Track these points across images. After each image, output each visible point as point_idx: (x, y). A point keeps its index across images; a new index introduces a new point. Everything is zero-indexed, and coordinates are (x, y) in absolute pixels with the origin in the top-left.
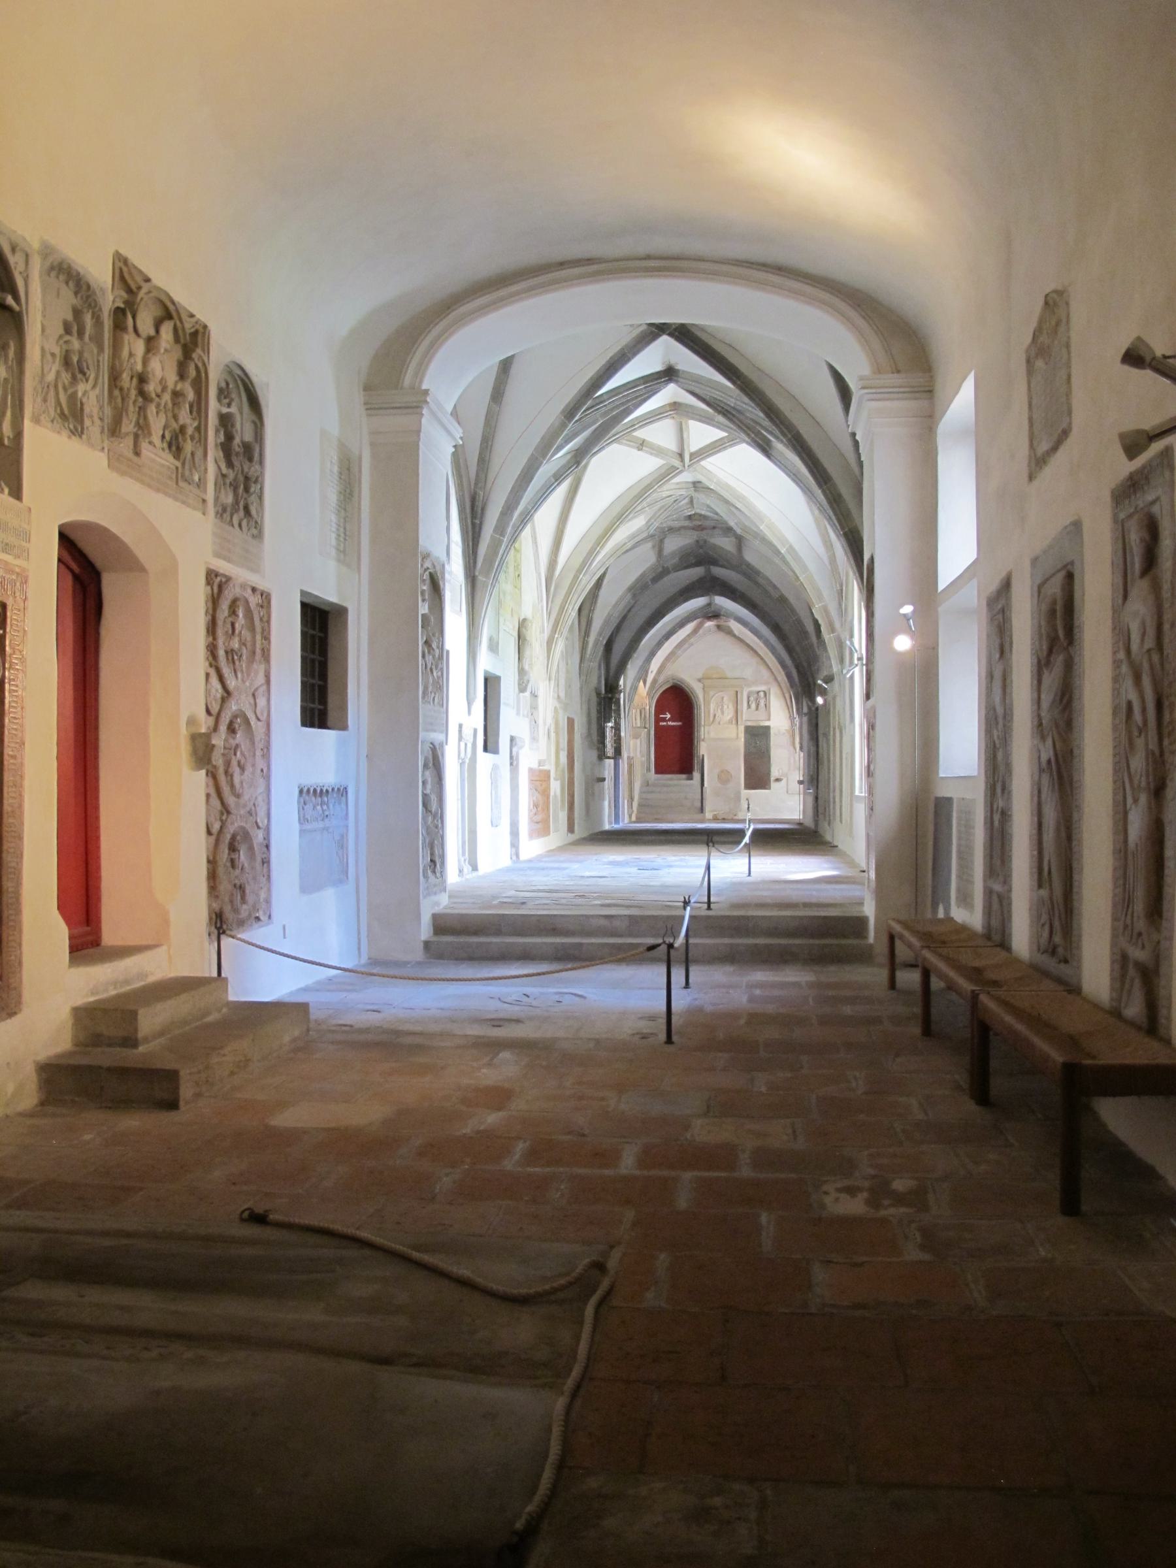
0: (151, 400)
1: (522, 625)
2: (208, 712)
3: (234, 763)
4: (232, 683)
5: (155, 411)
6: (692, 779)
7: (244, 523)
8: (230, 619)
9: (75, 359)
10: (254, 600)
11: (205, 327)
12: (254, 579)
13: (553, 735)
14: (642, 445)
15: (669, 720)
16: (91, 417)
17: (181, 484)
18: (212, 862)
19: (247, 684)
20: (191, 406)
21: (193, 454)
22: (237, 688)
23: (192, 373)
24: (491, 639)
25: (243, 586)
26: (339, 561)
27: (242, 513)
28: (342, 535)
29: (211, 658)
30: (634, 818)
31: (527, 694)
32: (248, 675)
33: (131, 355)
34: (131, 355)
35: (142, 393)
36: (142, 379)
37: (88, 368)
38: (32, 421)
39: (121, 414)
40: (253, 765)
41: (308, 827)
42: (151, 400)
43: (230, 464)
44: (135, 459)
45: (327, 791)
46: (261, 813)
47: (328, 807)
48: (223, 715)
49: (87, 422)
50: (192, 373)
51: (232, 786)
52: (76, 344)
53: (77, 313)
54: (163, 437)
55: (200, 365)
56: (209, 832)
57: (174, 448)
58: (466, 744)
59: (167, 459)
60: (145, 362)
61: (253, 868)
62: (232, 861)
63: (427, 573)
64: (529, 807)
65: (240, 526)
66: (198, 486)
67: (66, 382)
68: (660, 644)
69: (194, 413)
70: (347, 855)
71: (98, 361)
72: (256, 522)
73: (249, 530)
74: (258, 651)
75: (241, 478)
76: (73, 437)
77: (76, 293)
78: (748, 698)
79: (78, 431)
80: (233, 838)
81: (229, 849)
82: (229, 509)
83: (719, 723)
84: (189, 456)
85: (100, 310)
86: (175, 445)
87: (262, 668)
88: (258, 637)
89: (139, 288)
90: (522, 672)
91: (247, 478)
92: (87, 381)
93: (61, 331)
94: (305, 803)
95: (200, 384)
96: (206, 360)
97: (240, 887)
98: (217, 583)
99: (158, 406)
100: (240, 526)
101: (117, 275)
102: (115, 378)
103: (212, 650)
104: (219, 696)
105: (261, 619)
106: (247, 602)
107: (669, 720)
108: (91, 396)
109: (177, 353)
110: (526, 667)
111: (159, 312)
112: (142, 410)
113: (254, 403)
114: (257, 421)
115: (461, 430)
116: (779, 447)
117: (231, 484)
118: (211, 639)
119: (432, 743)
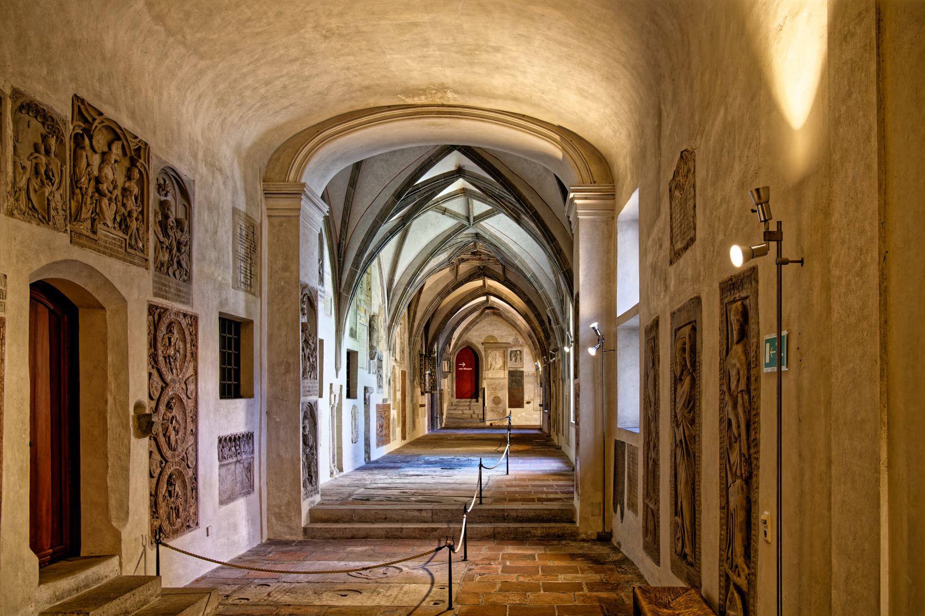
0: (105, 196)
1: (372, 319)
2: (151, 397)
3: (171, 428)
4: (169, 377)
5: (107, 202)
8: (167, 336)
9: (42, 170)
10: (184, 323)
11: (146, 144)
12: (183, 308)
15: (465, 367)
16: (56, 209)
17: (128, 250)
18: (154, 496)
19: (180, 376)
21: (138, 229)
22: (173, 381)
23: (136, 175)
24: (351, 329)
25: (177, 313)
26: (246, 291)
27: (175, 266)
28: (249, 275)
29: (153, 363)
31: (376, 360)
32: (181, 370)
33: (88, 165)
35: (98, 190)
36: (98, 181)
37: (53, 176)
40: (185, 428)
41: (226, 462)
42: (105, 196)
43: (166, 235)
44: (92, 236)
45: (239, 437)
46: (191, 459)
48: (162, 398)
49: (53, 213)
50: (136, 175)
51: (169, 444)
52: (43, 159)
53: (44, 138)
54: (115, 219)
55: (142, 170)
56: (151, 476)
57: (123, 227)
58: (335, 395)
61: (185, 494)
62: (170, 492)
65: (174, 275)
66: (143, 251)
68: (458, 324)
69: (139, 202)
71: (62, 170)
72: (186, 271)
73: (181, 277)
74: (188, 354)
75: (174, 244)
76: (41, 224)
77: (43, 124)
79: (45, 219)
80: (170, 476)
81: (167, 484)
82: (166, 264)
84: (135, 231)
85: (63, 135)
86: (123, 224)
87: (192, 365)
88: (188, 345)
89: (94, 120)
90: (372, 347)
91: (179, 243)
92: (53, 185)
93: (33, 151)
94: (223, 447)
95: (142, 182)
97: (175, 508)
98: (156, 314)
99: (110, 200)
100: (174, 275)
102: (75, 182)
103: (153, 358)
104: (159, 387)
105: (191, 334)
106: (180, 323)
107: (465, 367)
109: (126, 163)
110: (375, 344)
111: (110, 137)
112: (98, 202)
113: (185, 194)
114: (186, 204)
117: (167, 247)
118: (153, 350)
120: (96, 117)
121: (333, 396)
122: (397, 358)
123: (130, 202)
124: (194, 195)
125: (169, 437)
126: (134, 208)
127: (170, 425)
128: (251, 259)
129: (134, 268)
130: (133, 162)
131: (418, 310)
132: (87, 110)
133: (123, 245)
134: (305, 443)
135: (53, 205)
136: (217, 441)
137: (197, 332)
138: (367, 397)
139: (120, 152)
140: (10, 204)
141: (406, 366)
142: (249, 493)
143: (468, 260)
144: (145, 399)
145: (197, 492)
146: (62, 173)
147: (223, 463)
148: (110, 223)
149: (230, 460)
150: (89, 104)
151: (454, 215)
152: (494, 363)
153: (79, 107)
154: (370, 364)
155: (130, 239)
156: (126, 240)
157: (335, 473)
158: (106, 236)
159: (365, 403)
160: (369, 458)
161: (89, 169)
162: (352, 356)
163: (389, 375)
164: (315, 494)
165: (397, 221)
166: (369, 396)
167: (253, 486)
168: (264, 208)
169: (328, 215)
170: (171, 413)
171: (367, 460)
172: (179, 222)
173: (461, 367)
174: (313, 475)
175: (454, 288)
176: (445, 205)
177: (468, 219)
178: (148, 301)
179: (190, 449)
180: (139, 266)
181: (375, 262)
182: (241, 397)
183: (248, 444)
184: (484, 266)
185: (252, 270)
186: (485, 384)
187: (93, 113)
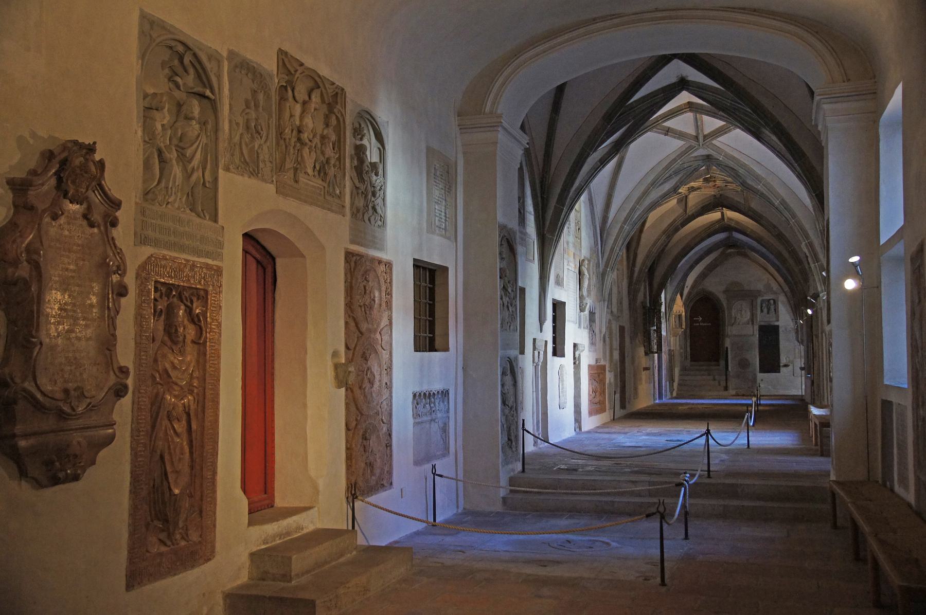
0: (306, 144)
2: (347, 347)
3: (366, 381)
5: (308, 150)
6: (719, 365)
7: (372, 219)
11: (343, 89)
13: (607, 339)
14: (668, 131)
16: (264, 161)
17: (328, 198)
20: (334, 144)
23: (333, 121)
27: (371, 211)
29: (349, 312)
30: (675, 394)
33: (291, 116)
34: (291, 116)
35: (299, 139)
37: (262, 130)
38: (224, 170)
39: (285, 159)
40: (380, 381)
44: (295, 185)
47: (435, 405)
49: (261, 166)
50: (333, 121)
52: (253, 115)
53: (254, 92)
54: (315, 167)
55: (339, 115)
57: (322, 174)
58: (539, 352)
59: (318, 182)
60: (302, 118)
63: (505, 239)
64: (589, 393)
66: (339, 197)
69: (336, 148)
70: (449, 437)
71: (268, 124)
72: (381, 216)
76: (252, 176)
78: (762, 304)
79: (255, 173)
81: (363, 438)
83: (739, 324)
85: (270, 89)
86: (322, 171)
89: (296, 71)
92: (261, 138)
94: (417, 404)
95: (339, 130)
96: (344, 113)
100: (369, 220)
101: (281, 63)
102: (280, 134)
103: (349, 306)
108: (264, 148)
109: (324, 110)
111: (311, 84)
115: (527, 138)
116: (767, 132)
119: (508, 358)
120: (298, 68)
121: (536, 353)
122: (613, 310)
123: (328, 149)
124: (388, 137)
126: (332, 155)
127: (365, 377)
128: (446, 200)
129: (331, 215)
130: (331, 109)
131: (638, 252)
132: (289, 61)
133: (322, 193)
134: (504, 403)
135: (261, 157)
136: (411, 396)
137: (391, 280)
138: (577, 356)
139: (319, 100)
140: (227, 159)
141: (625, 321)
143: (699, 188)
145: (391, 449)
146: (269, 126)
147: (417, 421)
148: (310, 171)
149: (425, 418)
150: (291, 56)
151: (680, 135)
152: (739, 316)
153: (283, 60)
154: (580, 317)
155: (329, 186)
156: (324, 187)
158: (307, 184)
159: (574, 363)
161: (292, 120)
162: (559, 307)
163: (604, 330)
164: (516, 461)
165: (609, 147)
166: (580, 355)
167: (449, 448)
168: (459, 143)
169: (528, 146)
172: (374, 166)
173: (697, 321)
174: (513, 438)
175: (684, 224)
176: (668, 124)
177: (697, 138)
178: (345, 248)
179: (385, 403)
180: (336, 213)
181: (584, 198)
182: (436, 351)
183: (443, 402)
184: (721, 195)
185: (447, 212)
186: (728, 343)
187: (296, 65)
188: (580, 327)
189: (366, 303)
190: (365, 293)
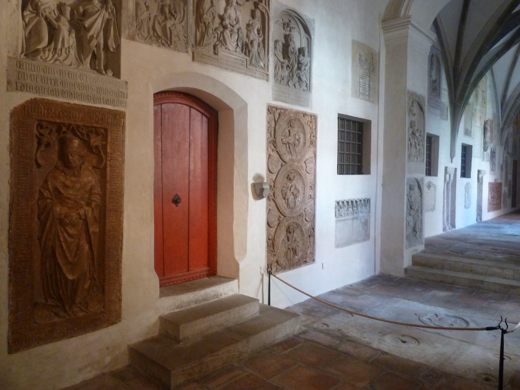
13: (504, 168)
40: (304, 194)
67: (160, 20)
92: (175, 19)
121: (448, 176)
125: (288, 200)
127: (288, 191)
128: (370, 77)
142: (364, 240)
144: (263, 172)
147: (339, 219)
149: (347, 217)
157: (448, 228)
159: (478, 181)
160: (481, 219)
166: (482, 177)
167: (369, 235)
170: (290, 183)
171: (479, 220)
188: (483, 160)
189: (291, 142)
190: (289, 135)
